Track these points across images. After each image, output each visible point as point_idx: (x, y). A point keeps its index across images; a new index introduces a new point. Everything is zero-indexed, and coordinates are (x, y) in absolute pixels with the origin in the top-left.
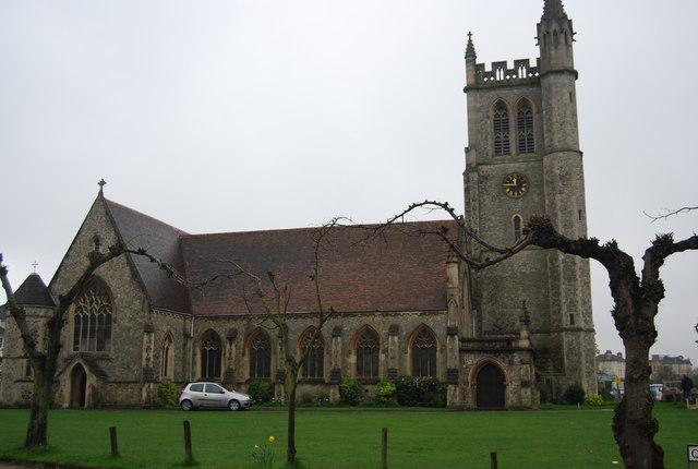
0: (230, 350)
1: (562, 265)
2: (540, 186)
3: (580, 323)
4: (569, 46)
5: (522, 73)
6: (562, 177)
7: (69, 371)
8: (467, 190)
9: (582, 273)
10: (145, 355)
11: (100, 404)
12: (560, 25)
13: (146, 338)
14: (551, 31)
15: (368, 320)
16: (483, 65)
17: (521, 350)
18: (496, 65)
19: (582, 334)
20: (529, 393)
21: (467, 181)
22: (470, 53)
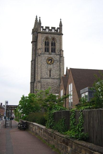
16: (43, 27)
18: (47, 27)
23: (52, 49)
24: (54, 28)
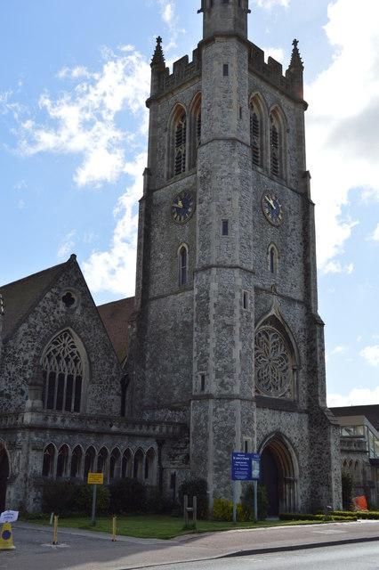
3: (213, 387)
9: (220, 312)
19: (211, 405)
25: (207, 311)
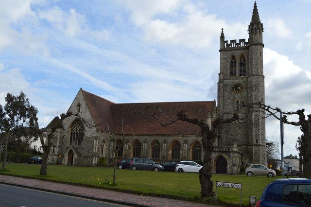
0: (126, 146)
1: (254, 120)
2: (247, 88)
3: (261, 143)
4: (261, 34)
5: (242, 45)
6: (255, 86)
7: (68, 153)
8: (219, 90)
10: (94, 147)
11: (79, 165)
12: (258, 26)
13: (95, 141)
14: (254, 28)
15: (176, 138)
16: (227, 41)
17: (234, 152)
18: (232, 41)
20: (236, 169)
21: (219, 86)
22: (222, 37)
23: (241, 71)
24: (244, 40)
25: (258, 123)
